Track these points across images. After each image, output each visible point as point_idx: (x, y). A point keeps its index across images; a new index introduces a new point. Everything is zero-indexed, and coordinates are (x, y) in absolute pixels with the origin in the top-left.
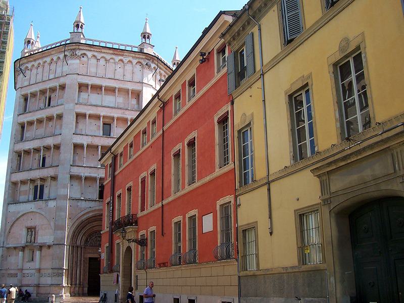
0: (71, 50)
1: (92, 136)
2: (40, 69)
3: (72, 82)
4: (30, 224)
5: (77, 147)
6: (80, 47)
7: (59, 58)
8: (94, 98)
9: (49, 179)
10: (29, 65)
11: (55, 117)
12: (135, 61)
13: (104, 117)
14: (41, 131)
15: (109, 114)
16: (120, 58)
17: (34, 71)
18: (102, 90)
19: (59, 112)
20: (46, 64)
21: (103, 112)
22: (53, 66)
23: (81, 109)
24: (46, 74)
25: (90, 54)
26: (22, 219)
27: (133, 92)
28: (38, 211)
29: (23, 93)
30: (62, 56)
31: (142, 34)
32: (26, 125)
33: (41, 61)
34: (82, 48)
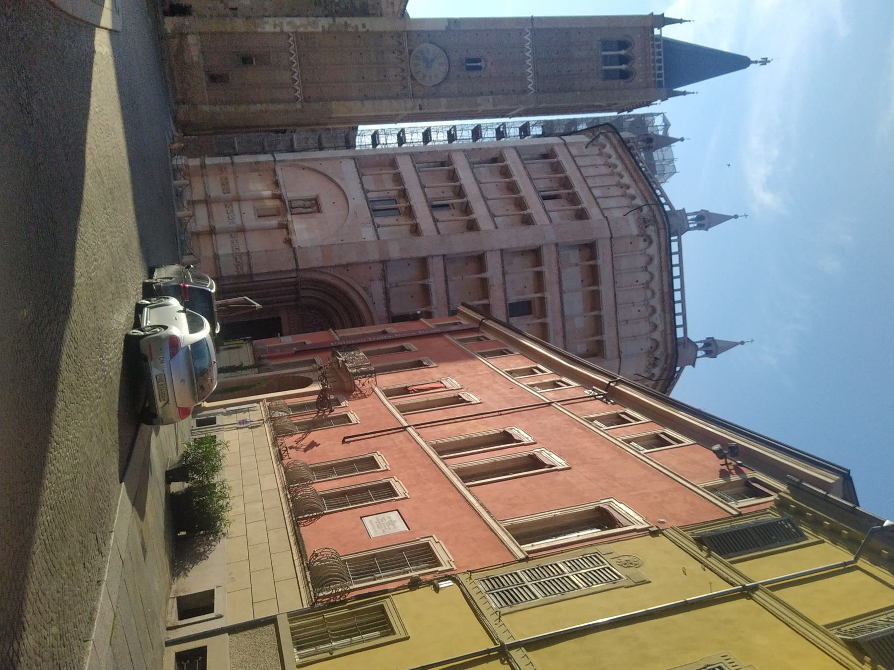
0: (654, 216)
1: (504, 284)
2: (605, 170)
4: (325, 202)
5: (479, 260)
6: (662, 232)
7: (633, 198)
8: (574, 275)
10: (608, 149)
11: (525, 212)
12: (657, 335)
13: (542, 300)
14: (493, 192)
15: (549, 307)
16: (658, 308)
17: (600, 161)
18: (589, 285)
19: (536, 218)
20: (616, 179)
21: (551, 295)
22: (616, 191)
23: (548, 256)
24: (599, 182)
25: (653, 250)
27: (600, 344)
29: (557, 149)
30: (639, 202)
31: (713, 338)
32: (501, 164)
33: (620, 168)
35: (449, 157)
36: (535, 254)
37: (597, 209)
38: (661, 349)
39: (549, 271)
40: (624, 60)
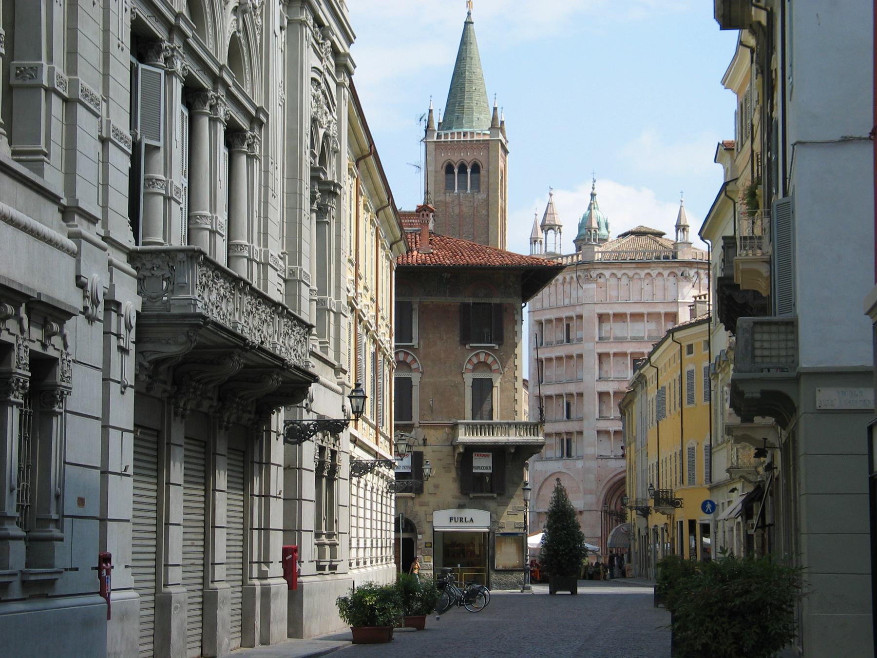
3: (590, 313)
7: (572, 278)
9: (575, 434)
12: (666, 273)
13: (631, 354)
16: (647, 271)
19: (579, 352)
21: (630, 348)
22: (567, 287)
24: (560, 297)
25: (607, 273)
28: (566, 471)
29: (537, 319)
30: (574, 276)
36: (602, 357)
37: (578, 307)
38: (675, 270)
39: (612, 349)
40: (463, 169)
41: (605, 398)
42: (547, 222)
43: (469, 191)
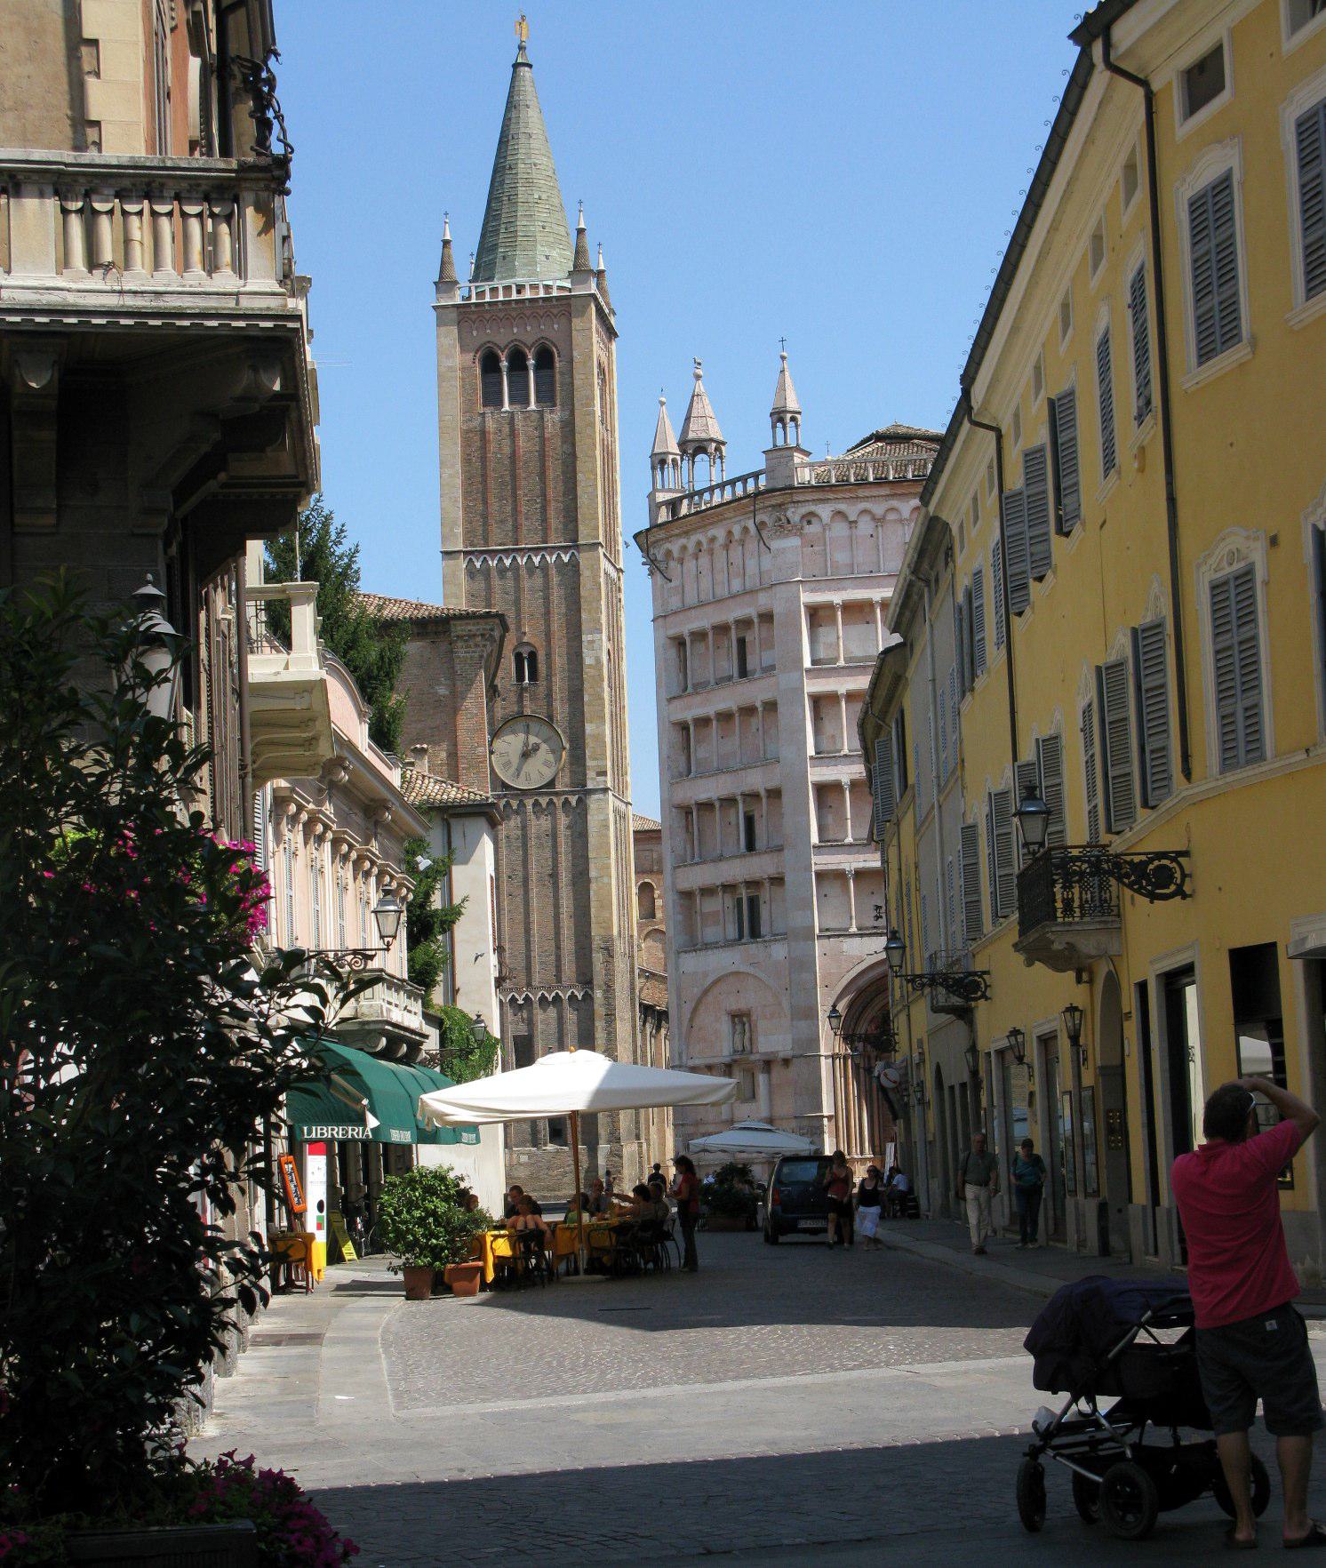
2: (704, 560)
7: (746, 530)
9: (767, 885)
10: (675, 547)
17: (690, 565)
19: (767, 696)
22: (736, 553)
24: (721, 577)
25: (825, 511)
26: (715, 991)
28: (751, 970)
29: (672, 632)
30: (750, 524)
34: (801, 498)
35: (678, 807)
40: (518, 361)
41: (831, 799)
42: (691, 435)
43: (533, 406)
